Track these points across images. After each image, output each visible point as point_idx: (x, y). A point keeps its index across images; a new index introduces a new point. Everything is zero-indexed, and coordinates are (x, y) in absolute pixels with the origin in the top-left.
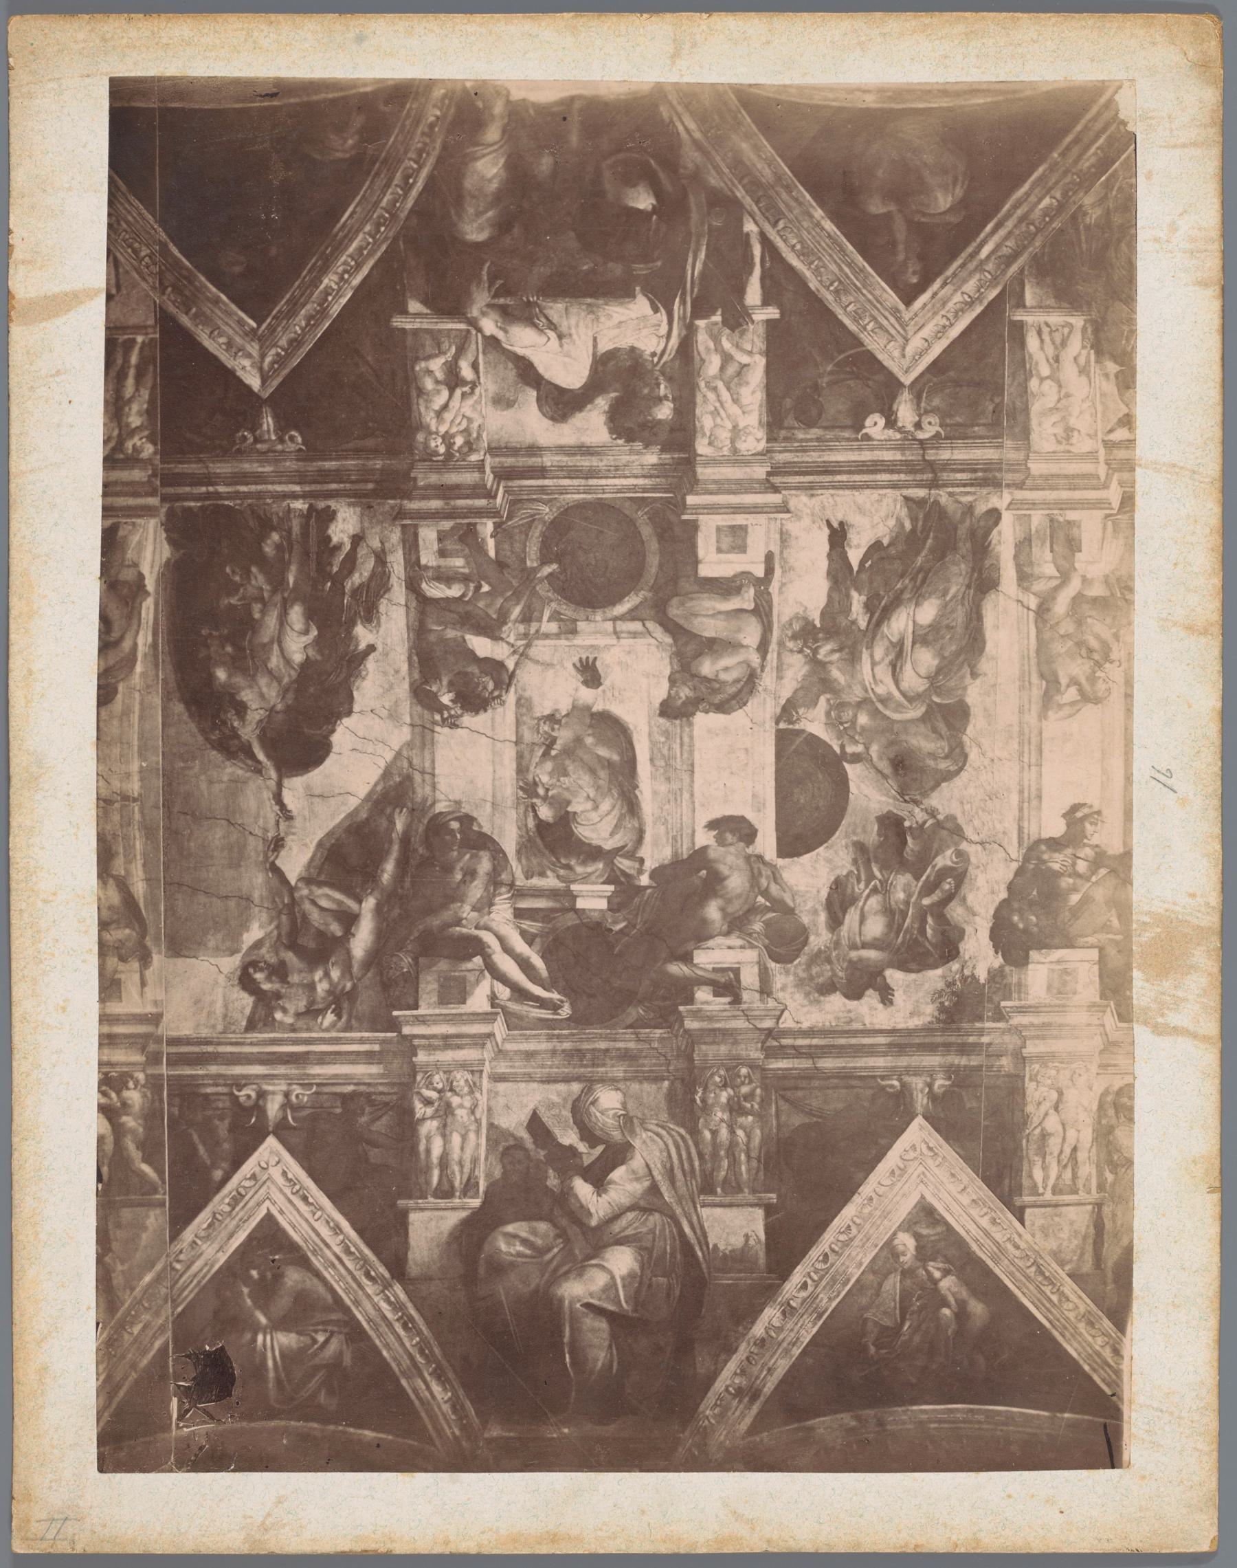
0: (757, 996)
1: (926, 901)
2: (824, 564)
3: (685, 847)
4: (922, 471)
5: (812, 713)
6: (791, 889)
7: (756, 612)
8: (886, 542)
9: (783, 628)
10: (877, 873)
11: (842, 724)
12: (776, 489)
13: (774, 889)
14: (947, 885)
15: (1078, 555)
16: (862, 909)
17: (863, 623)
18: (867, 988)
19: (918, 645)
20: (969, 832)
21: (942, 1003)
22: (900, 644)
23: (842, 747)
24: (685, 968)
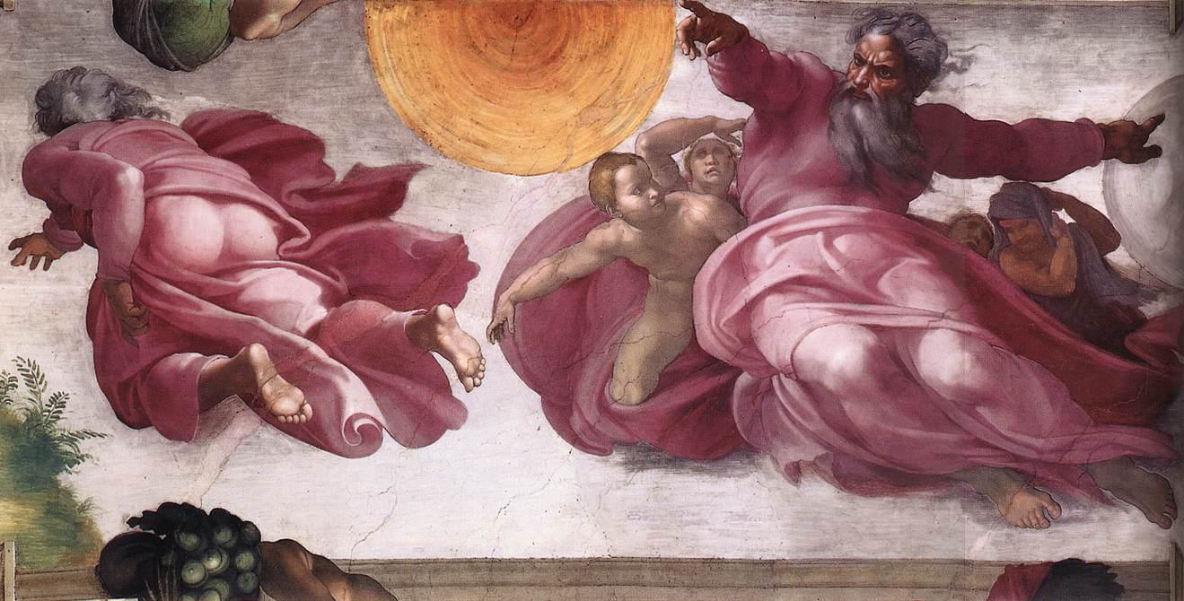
1: (258, 352)
2: (1066, 111)
8: (1118, 257)
10: (326, 239)
18: (49, 206)
19: (870, 338)
23: (631, 159)
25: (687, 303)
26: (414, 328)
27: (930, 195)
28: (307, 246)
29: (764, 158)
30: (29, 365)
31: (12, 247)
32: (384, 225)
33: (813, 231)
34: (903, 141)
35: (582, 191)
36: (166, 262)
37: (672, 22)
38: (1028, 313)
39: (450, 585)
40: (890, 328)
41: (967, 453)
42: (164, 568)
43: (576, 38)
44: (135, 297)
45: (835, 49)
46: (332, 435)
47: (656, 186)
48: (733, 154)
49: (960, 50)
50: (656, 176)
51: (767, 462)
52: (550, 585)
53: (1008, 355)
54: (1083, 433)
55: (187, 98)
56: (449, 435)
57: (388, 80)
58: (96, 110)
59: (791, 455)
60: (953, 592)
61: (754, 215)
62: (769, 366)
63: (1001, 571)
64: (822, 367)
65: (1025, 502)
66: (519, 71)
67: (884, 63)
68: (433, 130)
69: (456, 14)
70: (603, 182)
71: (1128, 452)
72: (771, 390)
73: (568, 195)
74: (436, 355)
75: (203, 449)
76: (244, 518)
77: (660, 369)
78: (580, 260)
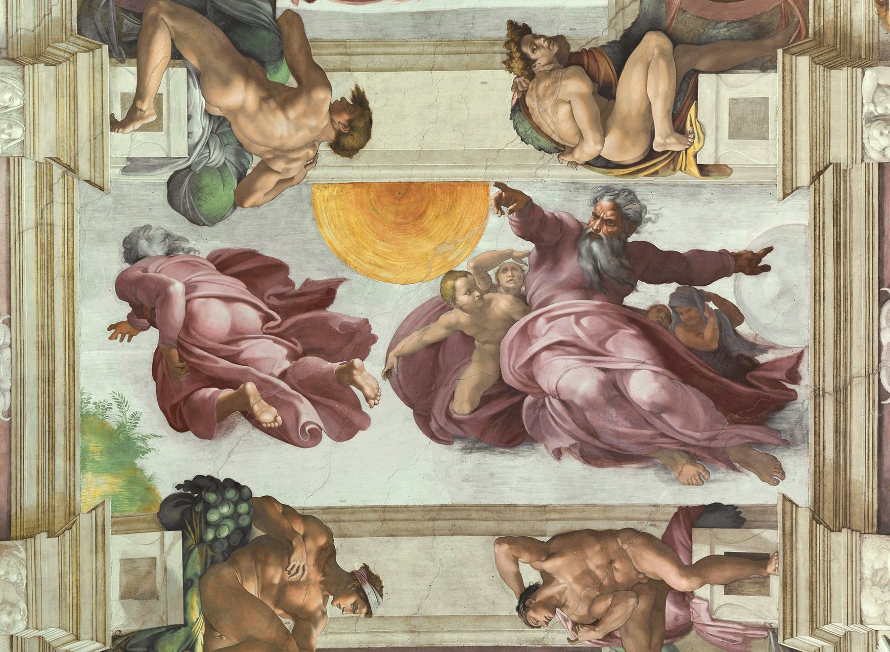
1: (250, 387)
2: (713, 246)
7: (651, 154)
12: (816, 177)
13: (270, 181)
15: (719, 589)
17: (631, 300)
18: (131, 306)
19: (601, 375)
23: (465, 274)
25: (496, 356)
26: (340, 371)
28: (279, 326)
29: (540, 274)
30: (119, 396)
31: (109, 329)
32: (323, 313)
33: (569, 314)
34: (620, 262)
35: (437, 293)
36: (198, 337)
37: (488, 195)
38: (691, 361)
39: (361, 521)
40: (613, 370)
41: (657, 441)
42: (197, 513)
43: (433, 204)
44: (180, 355)
45: (582, 210)
46: (293, 436)
47: (478, 289)
48: (523, 271)
49: (654, 210)
50: (479, 284)
51: (541, 447)
52: (418, 520)
53: (680, 384)
54: (723, 429)
55: (210, 242)
56: (360, 433)
57: (325, 230)
58: (158, 250)
59: (555, 444)
60: (650, 523)
61: (534, 307)
62: (543, 392)
63: (676, 510)
64: (573, 392)
65: (690, 470)
66: (401, 224)
67: (610, 218)
68: (351, 258)
69: (365, 191)
70: (449, 288)
71: (748, 441)
72: (544, 405)
73: (428, 297)
74: (353, 387)
75: (219, 443)
76: (243, 484)
77: (481, 394)
78: (435, 332)
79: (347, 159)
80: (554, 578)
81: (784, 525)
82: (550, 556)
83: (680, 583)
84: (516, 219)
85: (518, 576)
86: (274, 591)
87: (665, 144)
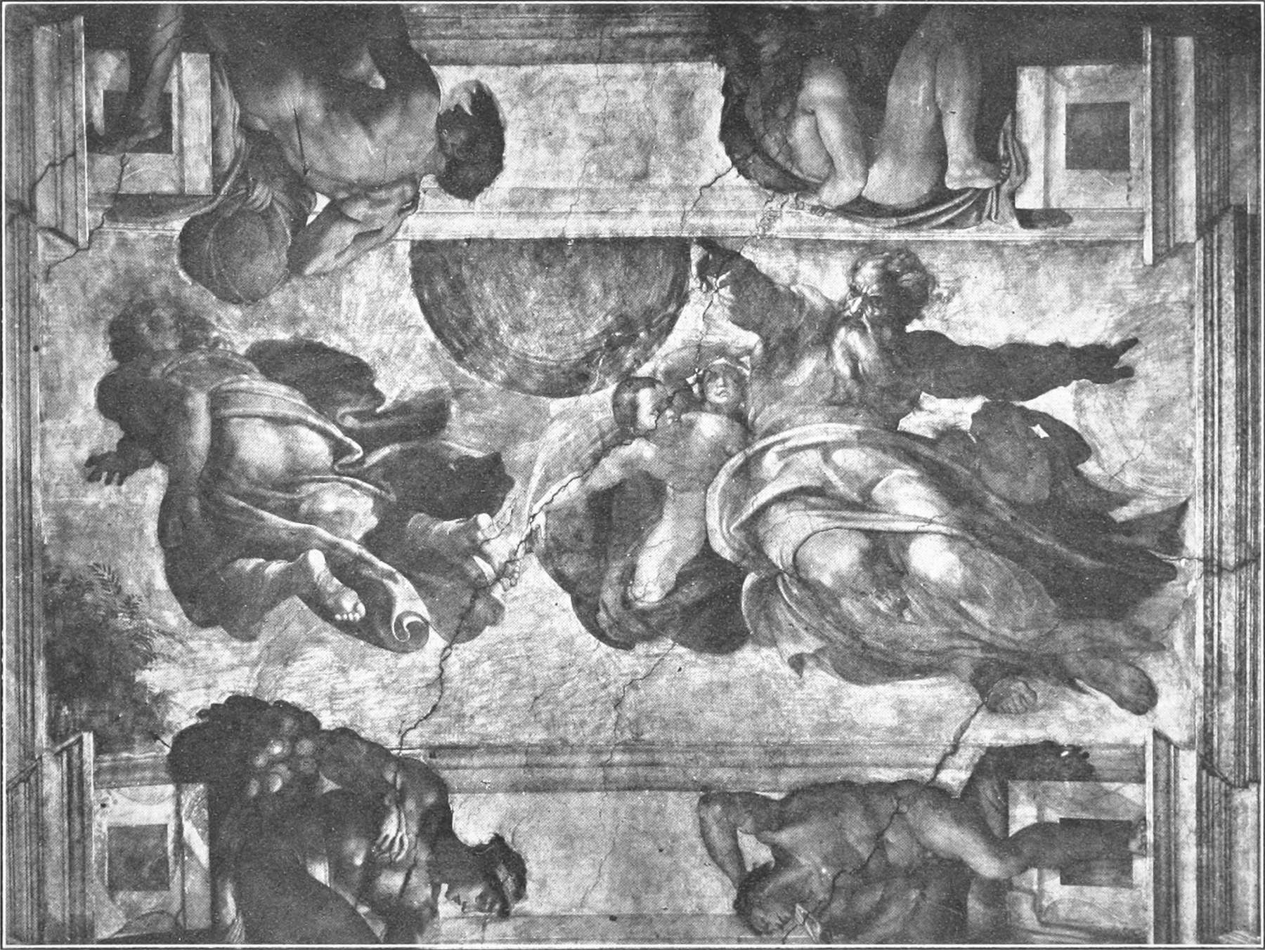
0: (107, 186)
1: (316, 560)
2: (1042, 337)
3: (434, 43)
4: (1240, 540)
5: (721, 315)
6: (346, 268)
7: (940, 195)
8: (1090, 468)
9: (904, 250)
10: (375, 458)
11: (699, 380)
12: (1206, 227)
14: (351, 605)
16: (299, 422)
17: (912, 423)
18: (122, 428)
19: (864, 543)
20: (466, 651)
21: (90, 588)
22: (866, 503)
23: (651, 382)
24: (169, 32)
27: (918, 413)
28: (361, 461)
61: (759, 432)
77: (678, 567)
79: (466, 202)
80: (791, 856)
81: (1155, 776)
82: (783, 823)
83: (986, 865)
84: (731, 296)
85: (737, 852)
86: (357, 877)
87: (962, 179)
